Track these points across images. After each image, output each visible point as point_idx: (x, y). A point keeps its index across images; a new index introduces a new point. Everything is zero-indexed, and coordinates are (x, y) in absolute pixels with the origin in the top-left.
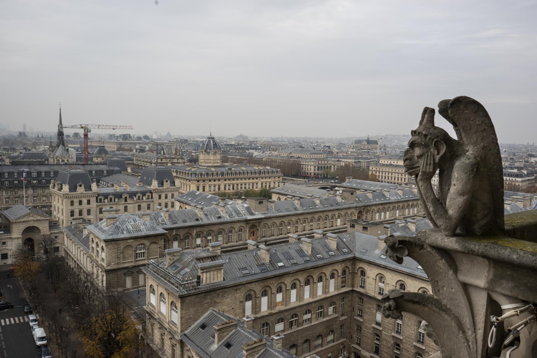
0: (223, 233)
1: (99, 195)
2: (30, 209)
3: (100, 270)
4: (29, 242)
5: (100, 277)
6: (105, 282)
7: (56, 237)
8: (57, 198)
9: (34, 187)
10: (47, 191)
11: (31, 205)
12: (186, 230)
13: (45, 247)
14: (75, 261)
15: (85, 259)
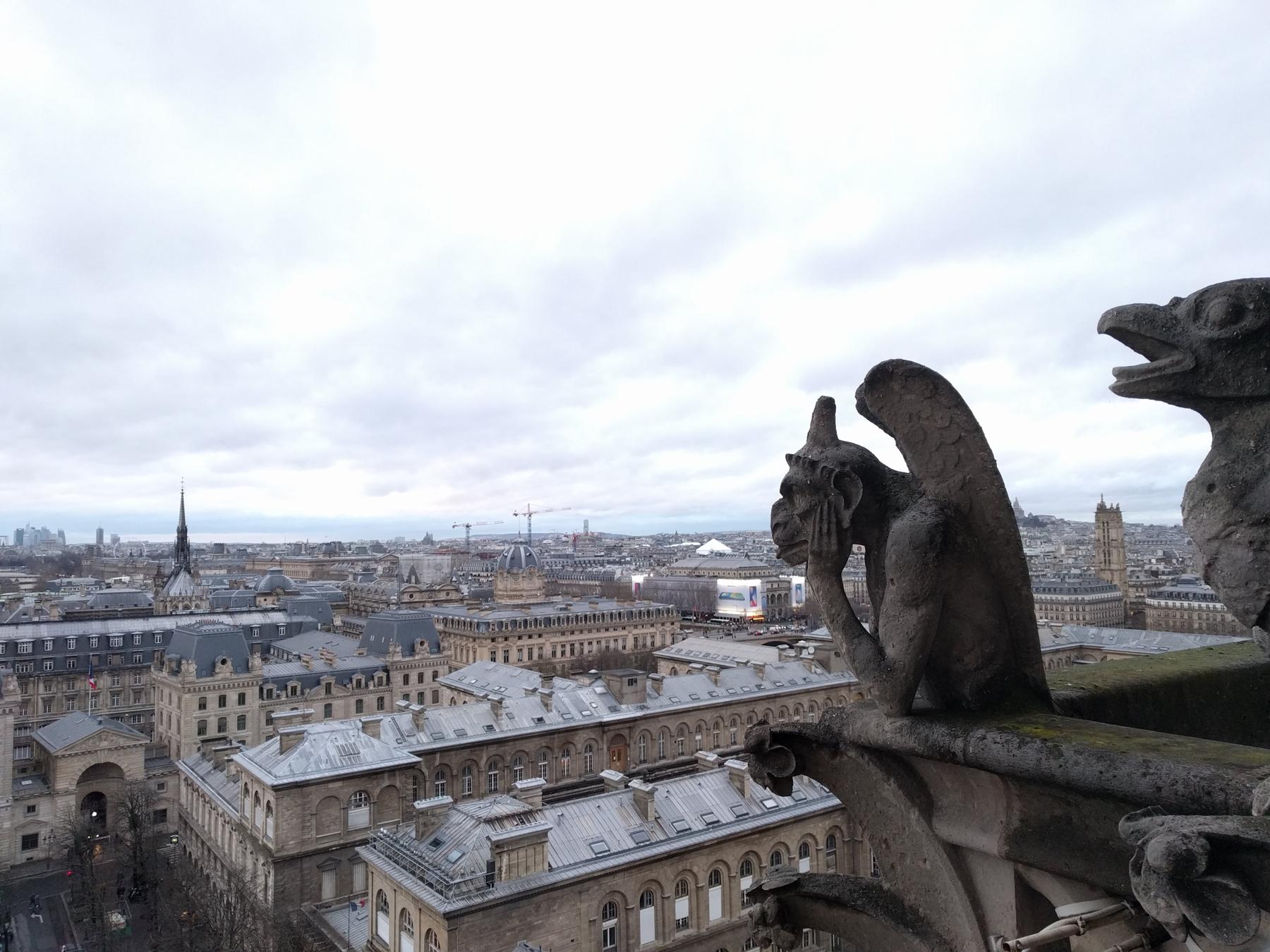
0: (549, 757)
1: (266, 681)
2: (100, 722)
3: (262, 861)
4: (94, 800)
5: (261, 880)
6: (270, 892)
7: (161, 786)
8: (166, 691)
9: (114, 671)
10: (144, 678)
11: (105, 711)
12: (465, 753)
13: (132, 811)
14: (203, 843)
15: (227, 835)
